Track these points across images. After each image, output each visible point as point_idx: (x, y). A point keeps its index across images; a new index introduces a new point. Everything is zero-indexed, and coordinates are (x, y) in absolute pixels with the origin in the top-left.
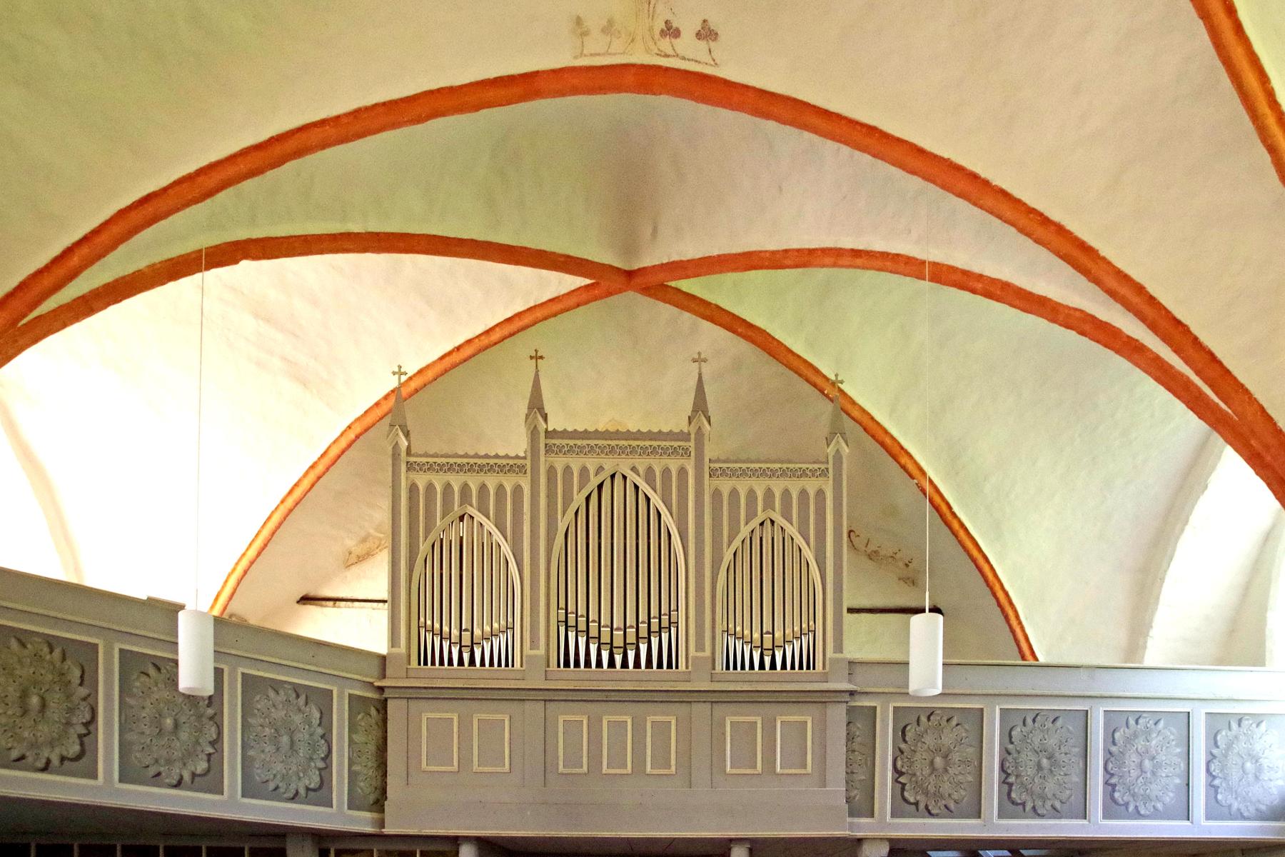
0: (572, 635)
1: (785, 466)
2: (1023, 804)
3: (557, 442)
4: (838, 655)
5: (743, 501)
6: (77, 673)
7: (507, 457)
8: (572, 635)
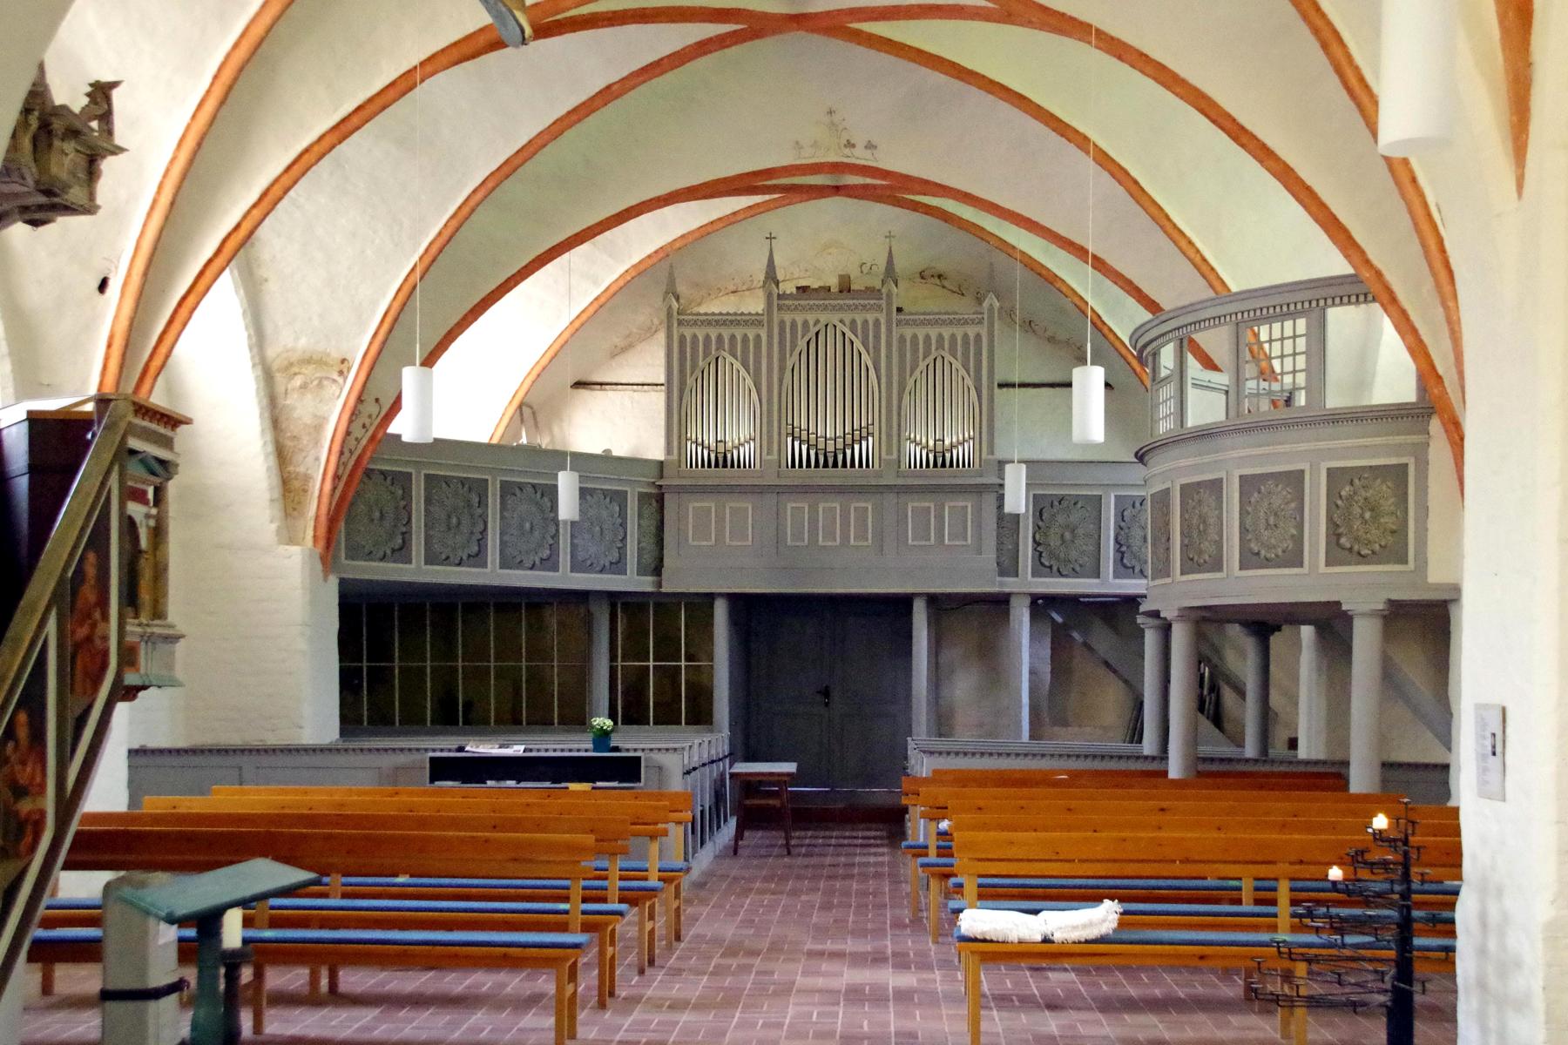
0: (797, 444)
1: (951, 317)
2: (1133, 568)
3: (787, 302)
4: (990, 457)
5: (921, 343)
6: (477, 500)
7: (750, 314)
8: (797, 444)
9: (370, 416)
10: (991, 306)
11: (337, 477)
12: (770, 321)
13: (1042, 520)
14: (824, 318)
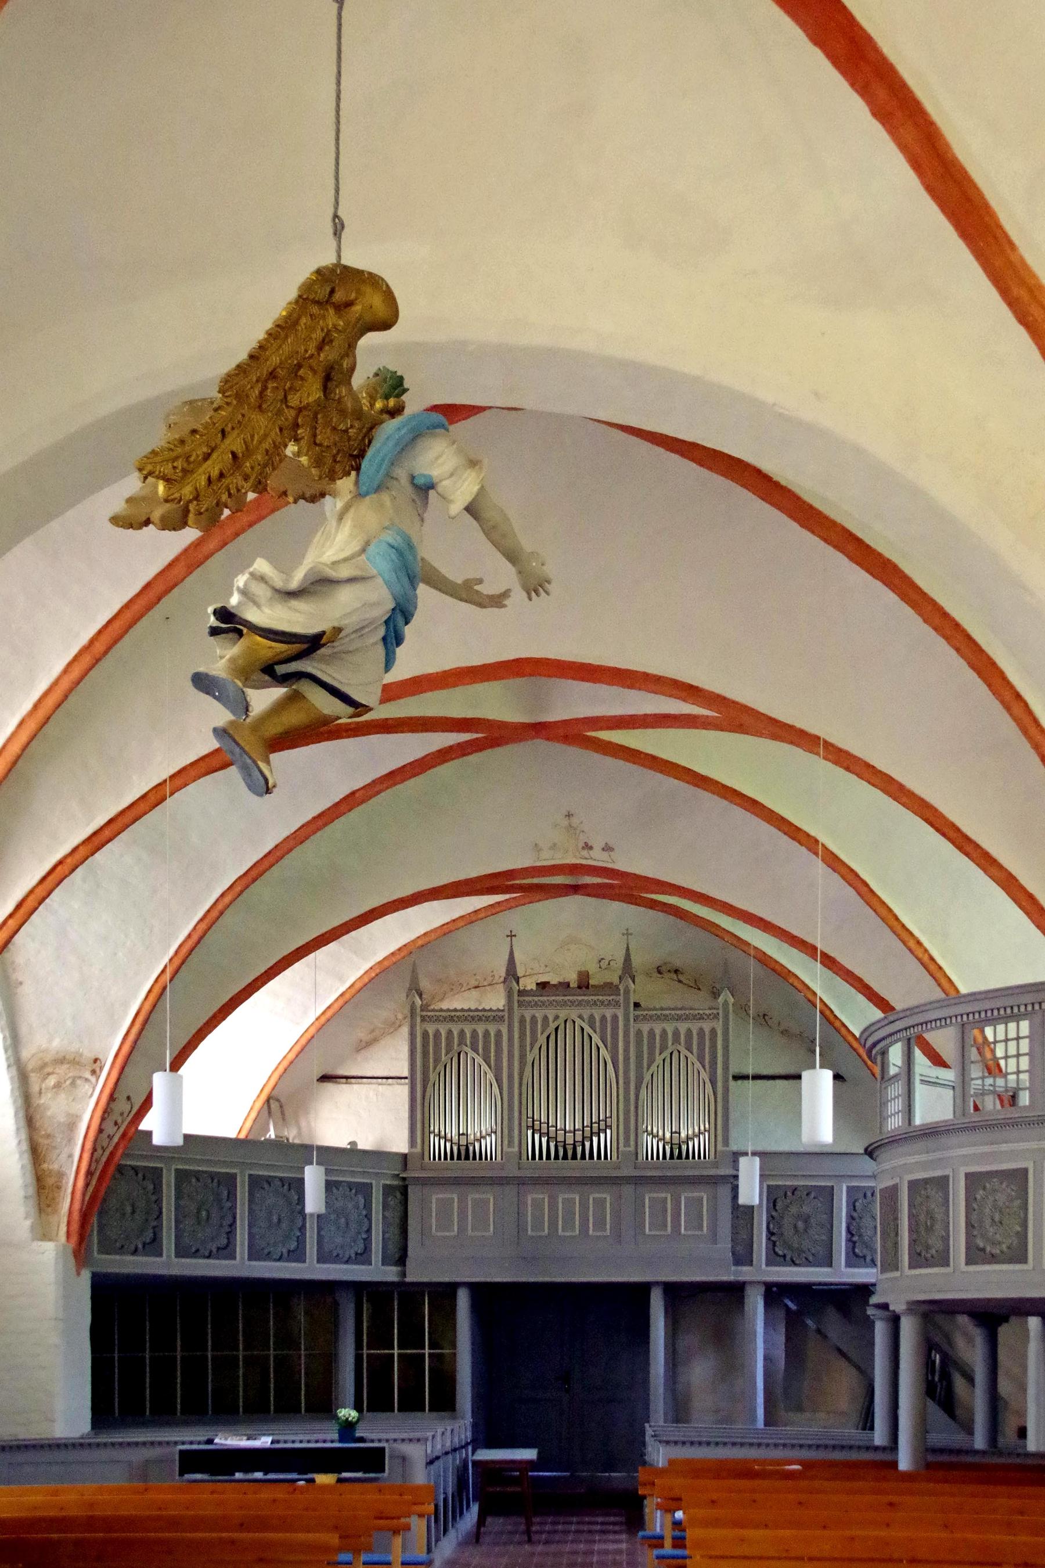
0: (537, 1136)
1: (687, 1012)
3: (527, 999)
4: (724, 1149)
5: (658, 1038)
6: (225, 1193)
7: (491, 1010)
8: (537, 1136)
9: (122, 1114)
10: (726, 1003)
11: (89, 1173)
12: (510, 1017)
13: (776, 1210)
14: (563, 1014)
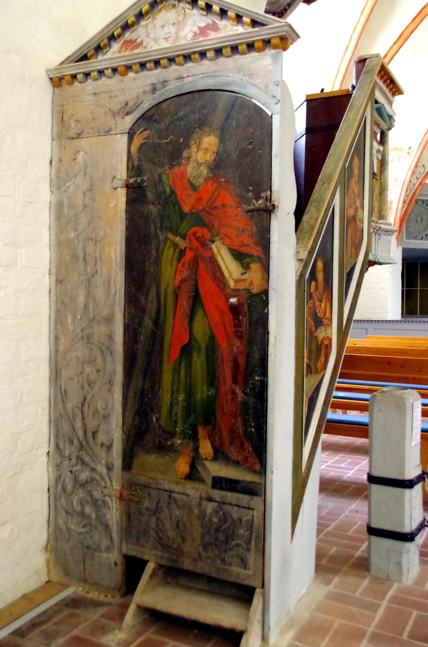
9: (420, 173)
11: (404, 202)
